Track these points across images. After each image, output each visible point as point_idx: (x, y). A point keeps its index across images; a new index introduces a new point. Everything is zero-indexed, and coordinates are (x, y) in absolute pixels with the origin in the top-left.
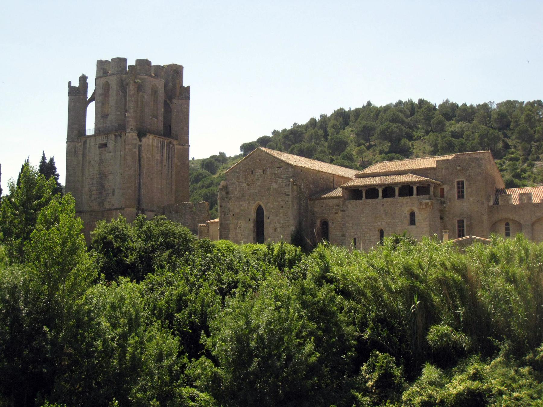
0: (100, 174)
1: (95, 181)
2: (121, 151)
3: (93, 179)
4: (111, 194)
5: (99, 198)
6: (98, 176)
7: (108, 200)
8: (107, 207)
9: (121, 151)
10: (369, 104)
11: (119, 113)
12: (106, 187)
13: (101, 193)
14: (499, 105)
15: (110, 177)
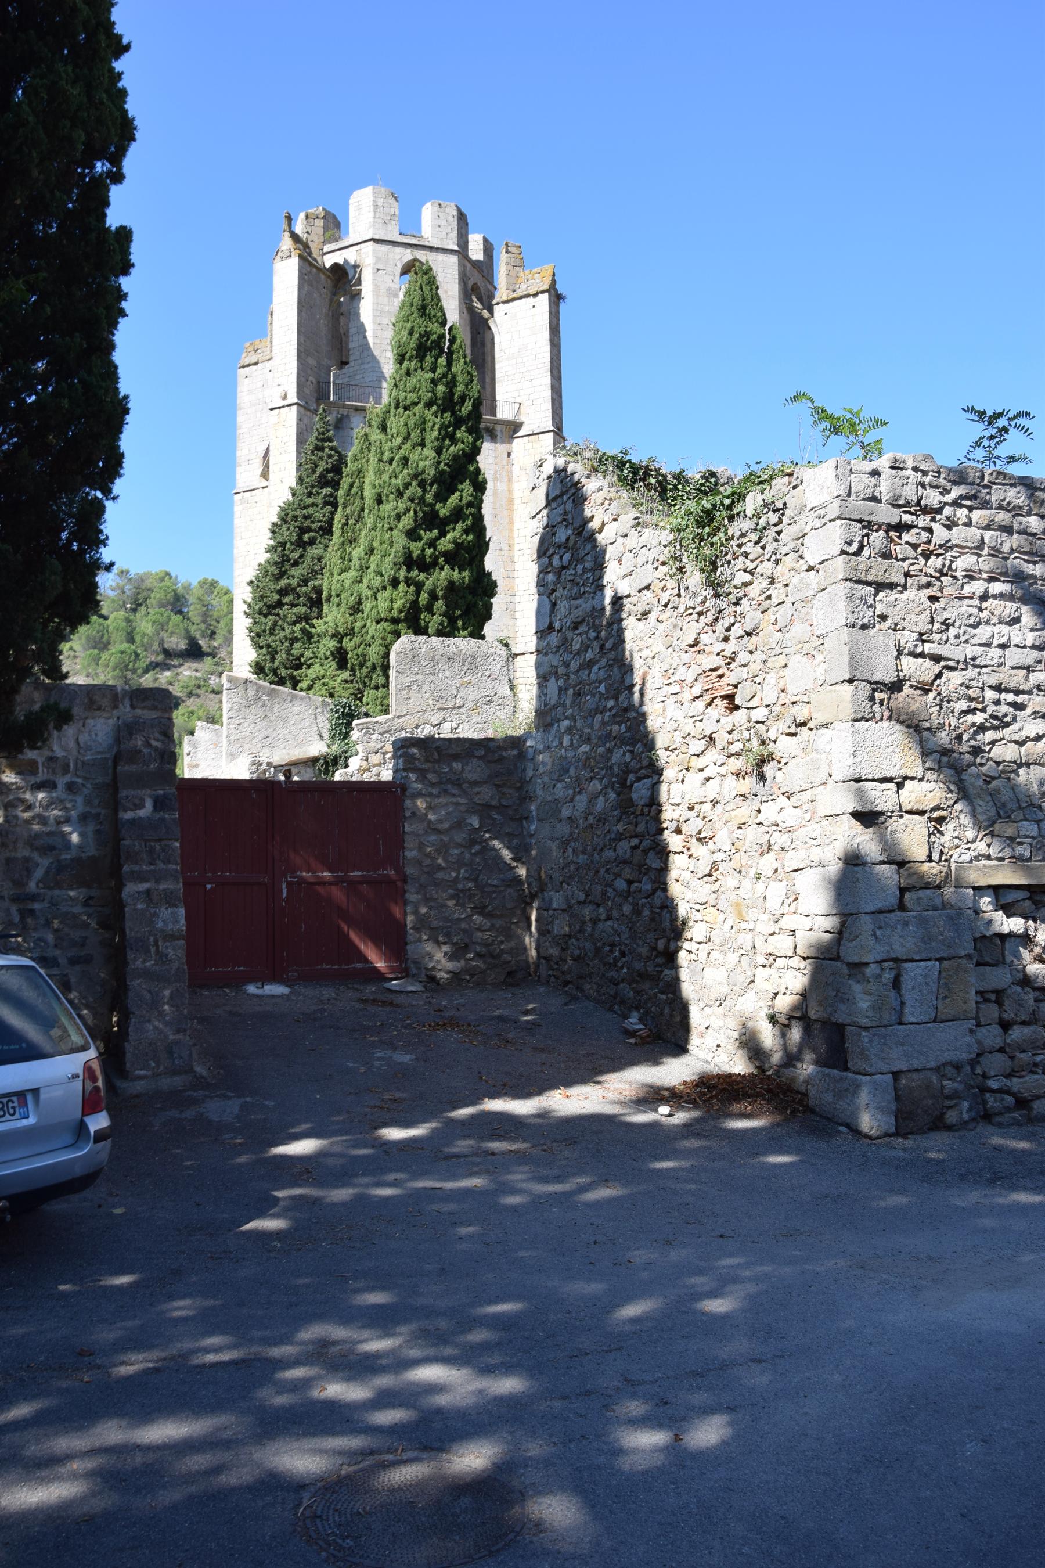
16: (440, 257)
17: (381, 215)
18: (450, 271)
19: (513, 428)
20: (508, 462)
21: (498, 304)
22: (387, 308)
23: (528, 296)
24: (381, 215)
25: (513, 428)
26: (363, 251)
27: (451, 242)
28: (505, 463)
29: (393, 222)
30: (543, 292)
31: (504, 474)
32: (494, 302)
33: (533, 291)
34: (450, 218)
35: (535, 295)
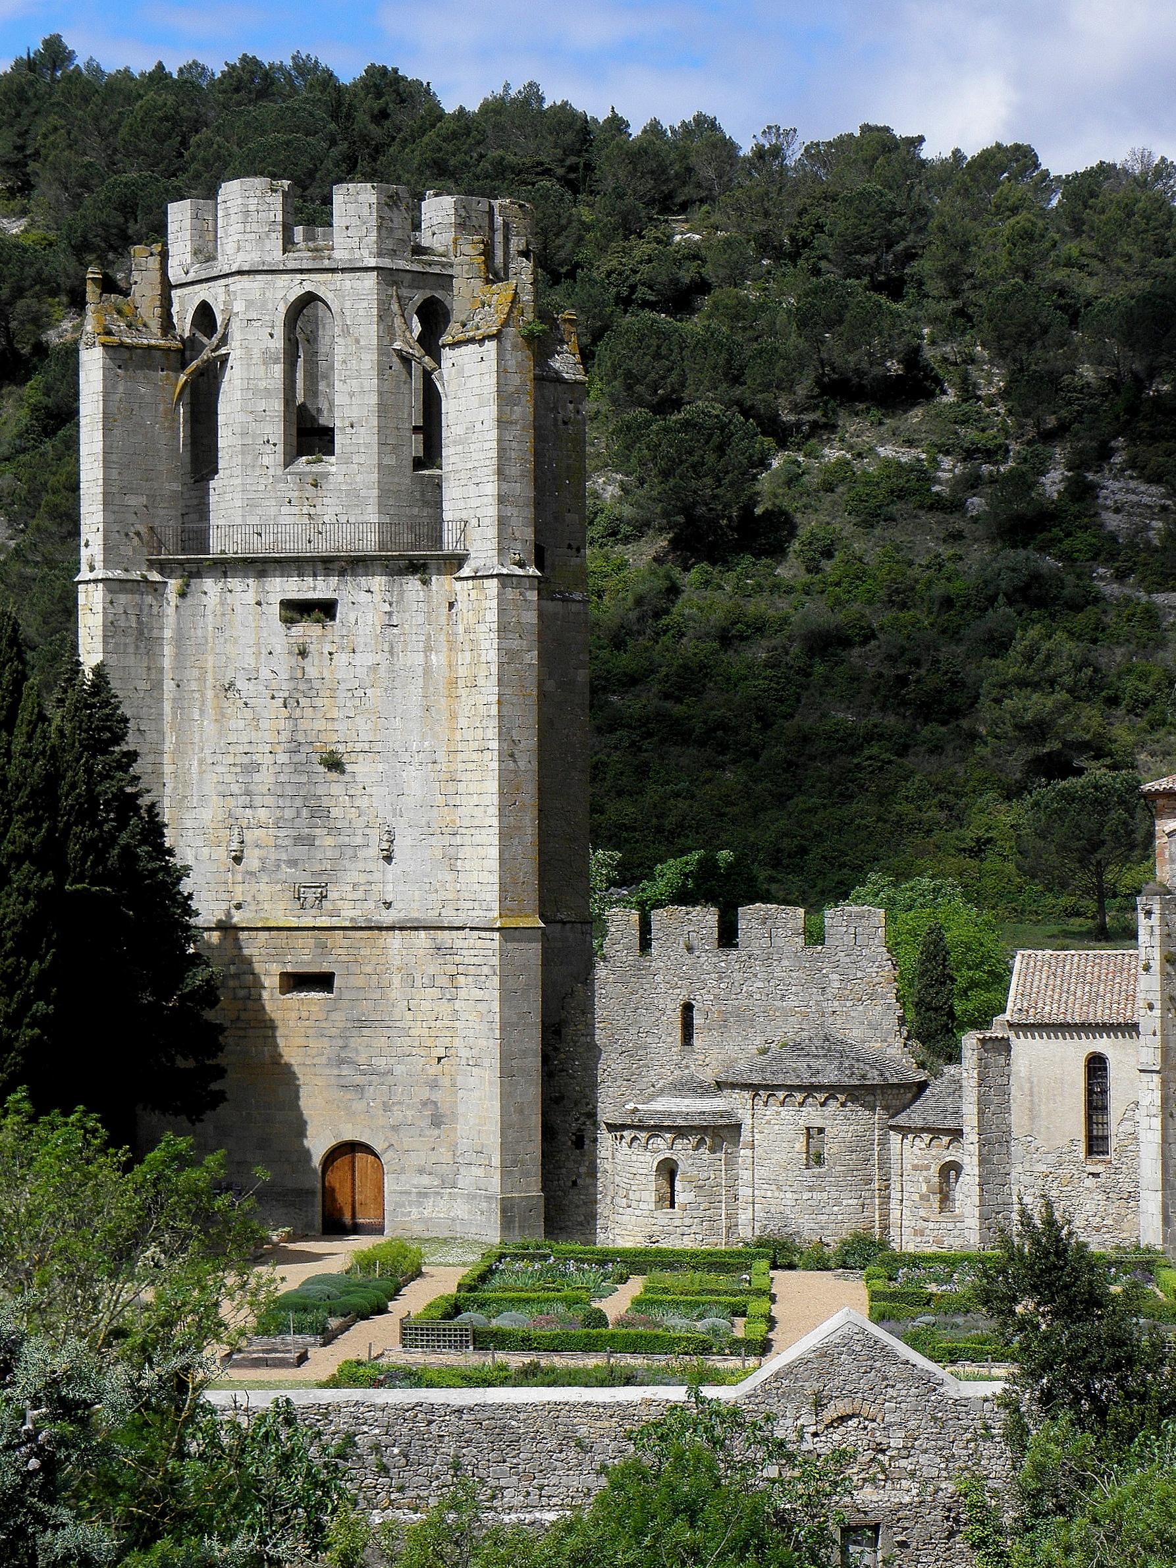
0: (295, 748)
1: (264, 779)
2: (428, 649)
3: (255, 767)
4: (374, 851)
5: (293, 863)
6: (283, 758)
7: (353, 876)
8: (349, 914)
9: (428, 649)
10: (55, 52)
11: (390, 460)
12: (335, 812)
13: (308, 841)
14: (813, 152)
15: (360, 768)
16: (346, 282)
17: (255, 227)
18: (365, 304)
19: (456, 561)
20: (449, 617)
21: (444, 346)
22: (262, 384)
23: (471, 341)
24: (255, 227)
25: (456, 561)
26: (232, 288)
27: (365, 253)
28: (443, 620)
29: (274, 235)
30: (490, 337)
31: (443, 638)
32: (446, 339)
33: (479, 334)
34: (365, 211)
35: (481, 341)
